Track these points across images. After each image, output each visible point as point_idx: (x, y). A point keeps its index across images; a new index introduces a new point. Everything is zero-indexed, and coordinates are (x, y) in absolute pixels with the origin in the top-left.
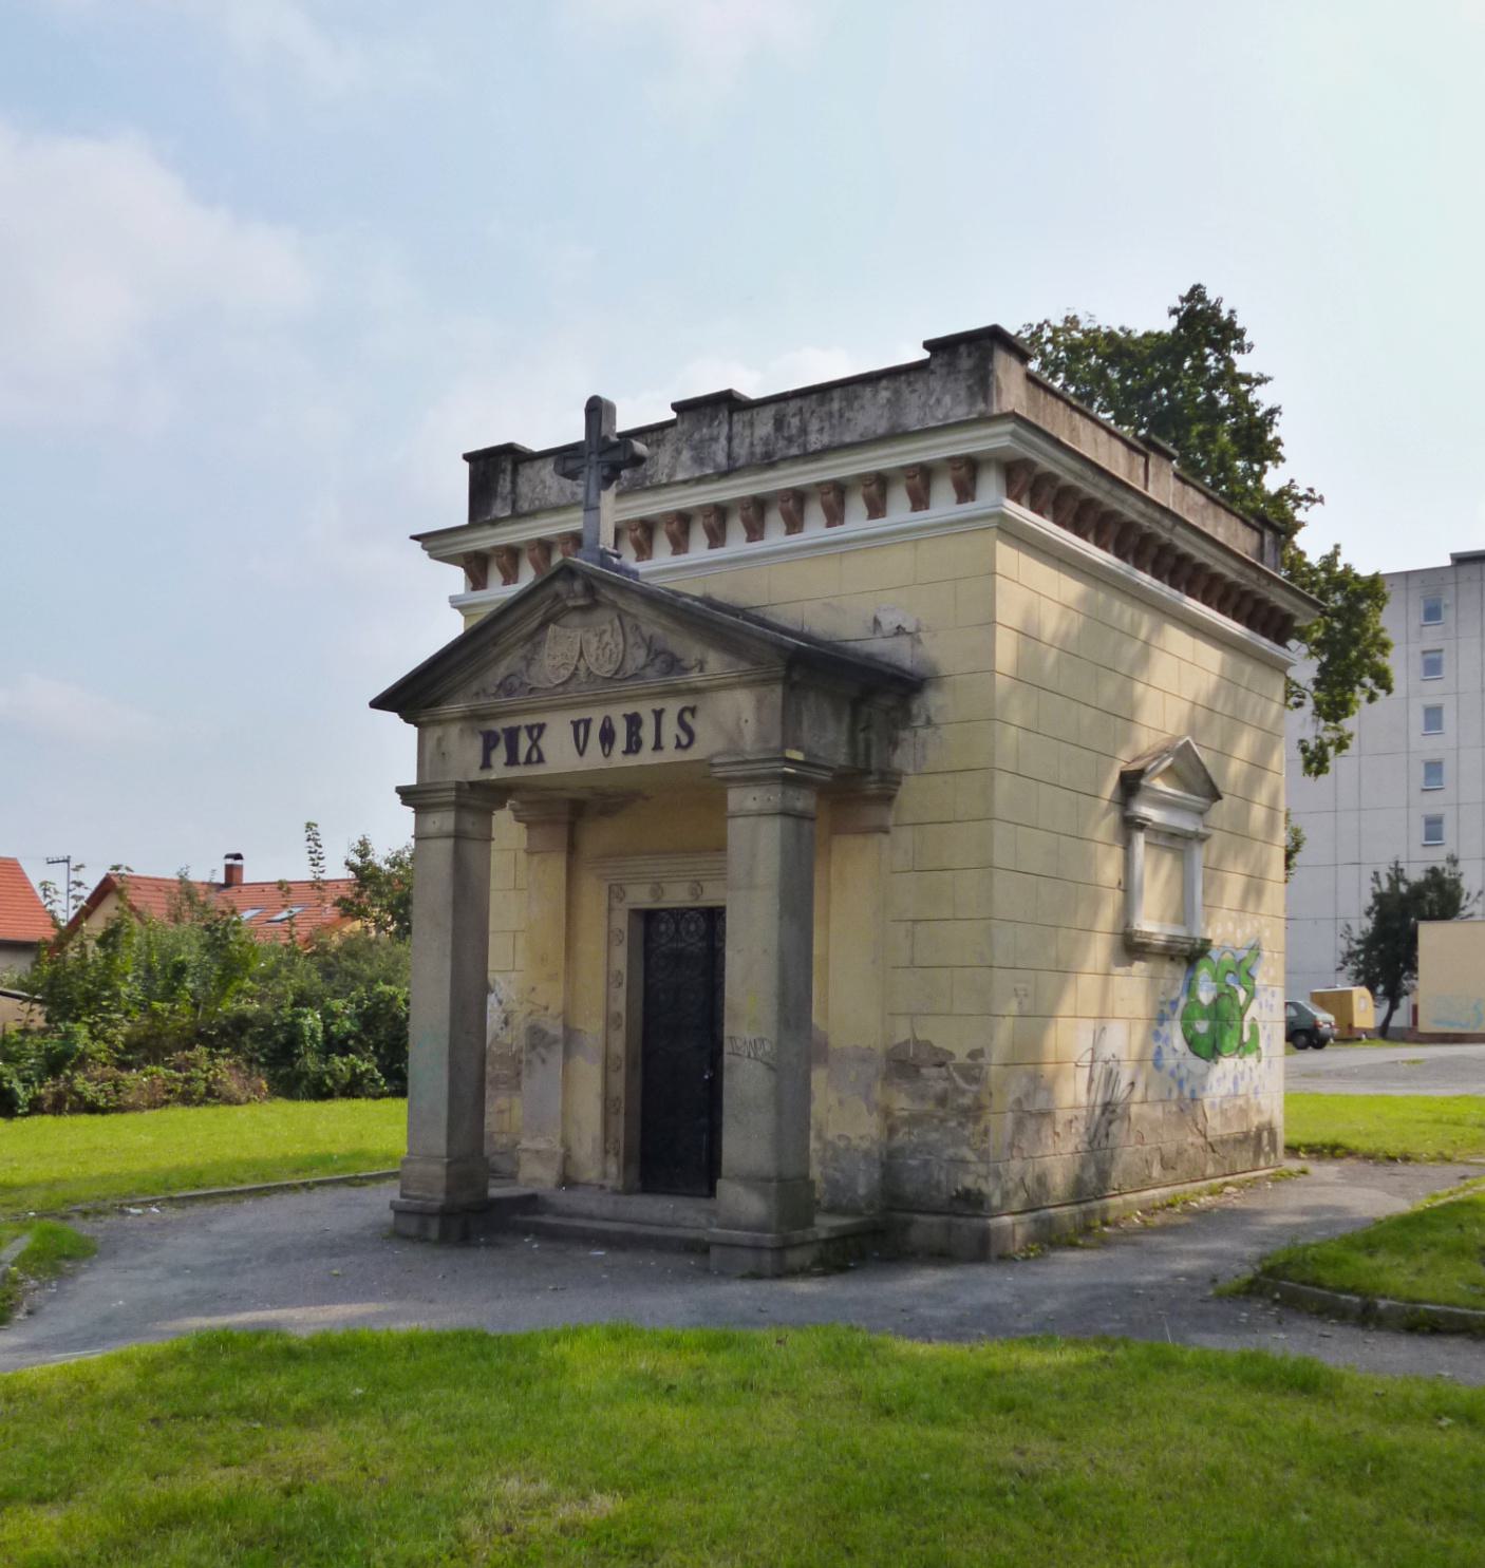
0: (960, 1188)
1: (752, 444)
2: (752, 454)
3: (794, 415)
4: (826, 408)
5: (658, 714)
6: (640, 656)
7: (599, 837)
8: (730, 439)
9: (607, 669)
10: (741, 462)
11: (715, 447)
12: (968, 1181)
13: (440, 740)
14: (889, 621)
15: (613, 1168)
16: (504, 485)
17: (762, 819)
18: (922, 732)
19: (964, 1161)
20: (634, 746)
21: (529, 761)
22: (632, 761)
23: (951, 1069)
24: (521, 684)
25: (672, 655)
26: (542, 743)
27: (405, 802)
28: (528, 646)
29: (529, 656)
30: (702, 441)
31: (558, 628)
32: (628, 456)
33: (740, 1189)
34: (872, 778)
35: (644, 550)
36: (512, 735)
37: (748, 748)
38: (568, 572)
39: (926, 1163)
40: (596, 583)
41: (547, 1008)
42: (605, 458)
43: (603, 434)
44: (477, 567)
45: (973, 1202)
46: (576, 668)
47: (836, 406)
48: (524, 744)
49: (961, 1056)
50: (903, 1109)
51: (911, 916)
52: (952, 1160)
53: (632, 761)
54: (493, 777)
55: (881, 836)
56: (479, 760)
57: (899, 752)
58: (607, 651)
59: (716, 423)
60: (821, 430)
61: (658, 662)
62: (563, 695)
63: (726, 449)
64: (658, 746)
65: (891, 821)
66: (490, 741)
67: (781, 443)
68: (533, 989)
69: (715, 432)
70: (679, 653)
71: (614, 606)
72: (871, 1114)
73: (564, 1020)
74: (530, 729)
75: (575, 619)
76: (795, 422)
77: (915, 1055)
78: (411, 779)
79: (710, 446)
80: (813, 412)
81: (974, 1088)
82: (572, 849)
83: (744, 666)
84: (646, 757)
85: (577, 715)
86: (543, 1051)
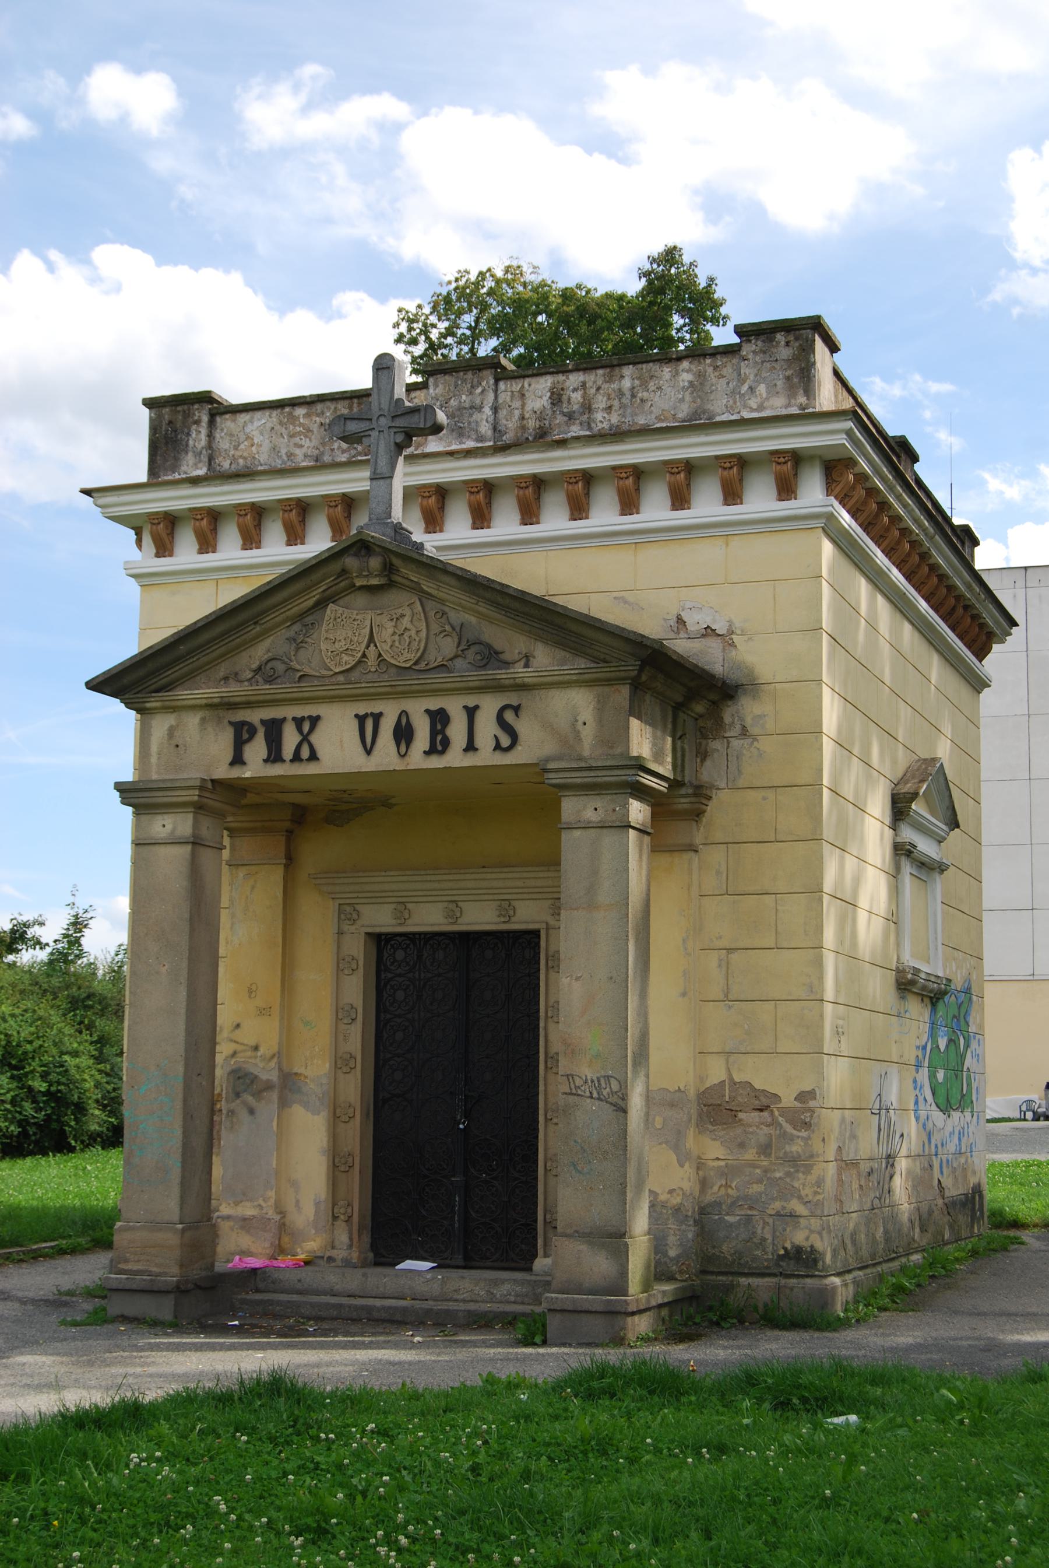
0: (788, 1246)
1: (522, 418)
2: (523, 428)
3: (575, 390)
4: (615, 386)
5: (471, 712)
6: (448, 646)
7: (320, 850)
8: (495, 409)
9: (406, 658)
10: (508, 438)
11: (476, 416)
12: (799, 1238)
13: (171, 732)
14: (696, 621)
15: (343, 1237)
16: (198, 438)
17: (605, 831)
18: (735, 743)
19: (793, 1215)
20: (439, 745)
21: (297, 758)
22: (436, 762)
23: (776, 1113)
24: (290, 669)
25: (489, 646)
26: (314, 738)
27: (125, 801)
28: (297, 627)
29: (301, 638)
30: (460, 408)
31: (340, 610)
32: (429, 425)
33: (584, 1247)
34: (683, 791)
35: (433, 522)
36: (274, 730)
37: (586, 753)
38: (362, 546)
39: (749, 1219)
40: (396, 561)
41: (256, 1048)
42: (399, 422)
43: (396, 397)
44: (160, 531)
45: (804, 1260)
46: (364, 655)
47: (627, 383)
48: (290, 738)
49: (788, 1099)
50: (718, 1159)
51: (724, 943)
52: (778, 1214)
53: (436, 762)
54: (248, 774)
55: (692, 854)
56: (229, 756)
57: (708, 763)
58: (406, 636)
59: (479, 390)
60: (609, 409)
61: (470, 654)
62: (344, 687)
63: (491, 419)
64: (471, 747)
65: (698, 839)
66: (242, 734)
67: (560, 419)
68: (238, 1026)
69: (478, 401)
70: (497, 645)
71: (416, 589)
72: (682, 1166)
73: (279, 1063)
74: (299, 722)
75: (360, 600)
76: (577, 397)
77: (733, 1099)
78: (128, 775)
79: (471, 415)
80: (598, 389)
81: (804, 1134)
82: (290, 861)
83: (582, 663)
84: (455, 758)
85: (362, 709)
86: (250, 1099)
